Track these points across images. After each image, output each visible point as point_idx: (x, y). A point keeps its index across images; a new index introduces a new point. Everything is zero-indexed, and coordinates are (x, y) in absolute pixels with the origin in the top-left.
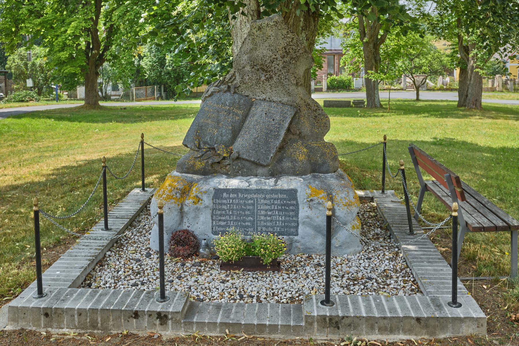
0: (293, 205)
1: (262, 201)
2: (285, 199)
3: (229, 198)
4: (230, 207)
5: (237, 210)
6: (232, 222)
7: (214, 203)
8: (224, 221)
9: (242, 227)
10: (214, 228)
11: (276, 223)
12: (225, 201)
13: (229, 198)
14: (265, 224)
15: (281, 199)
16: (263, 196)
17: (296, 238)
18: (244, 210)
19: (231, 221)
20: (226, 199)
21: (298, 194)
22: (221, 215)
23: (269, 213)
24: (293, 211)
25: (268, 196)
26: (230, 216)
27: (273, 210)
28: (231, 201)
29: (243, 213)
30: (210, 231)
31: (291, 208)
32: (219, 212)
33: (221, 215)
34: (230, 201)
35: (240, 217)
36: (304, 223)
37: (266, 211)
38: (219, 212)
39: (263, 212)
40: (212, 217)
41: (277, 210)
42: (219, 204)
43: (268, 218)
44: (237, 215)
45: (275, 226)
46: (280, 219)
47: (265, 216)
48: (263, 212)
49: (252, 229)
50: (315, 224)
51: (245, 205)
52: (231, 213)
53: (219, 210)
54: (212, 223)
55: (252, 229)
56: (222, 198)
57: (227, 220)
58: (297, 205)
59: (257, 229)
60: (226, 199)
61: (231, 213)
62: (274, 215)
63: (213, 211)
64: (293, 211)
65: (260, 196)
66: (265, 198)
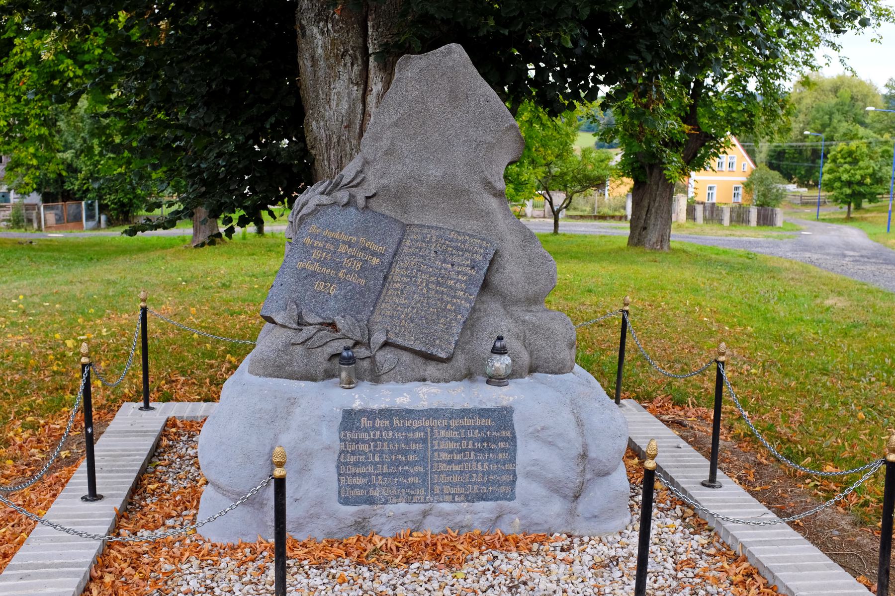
0: (505, 439)
1: (443, 432)
2: (489, 428)
3: (374, 428)
4: (375, 446)
5: (391, 452)
6: (380, 478)
7: (341, 440)
8: (364, 475)
9: (401, 485)
10: (343, 491)
11: (471, 477)
12: (364, 436)
13: (374, 428)
14: (449, 479)
15: (481, 428)
16: (445, 423)
17: (511, 504)
18: (405, 453)
19: (377, 475)
20: (366, 430)
21: (516, 417)
22: (356, 464)
23: (458, 457)
24: (504, 450)
25: (453, 423)
26: (375, 464)
27: (465, 450)
28: (378, 433)
29: (404, 458)
30: (335, 497)
31: (501, 445)
32: (353, 459)
33: (356, 464)
34: (374, 435)
35: (397, 467)
36: (528, 475)
37: (451, 452)
38: (353, 459)
39: (445, 456)
40: (338, 467)
41: (474, 450)
42: (352, 440)
43: (456, 468)
44: (391, 464)
45: (469, 483)
46: (480, 468)
47: (450, 462)
48: (445, 456)
49: (423, 490)
50: (550, 476)
51: (407, 441)
52: (377, 459)
53: (353, 453)
54: (339, 480)
55: (423, 490)
56: (358, 429)
57: (370, 474)
58: (514, 438)
59: (432, 489)
60: (366, 430)
61: (377, 459)
62: (466, 461)
63: (339, 456)
64: (504, 450)
65: (437, 423)
66: (448, 428)
